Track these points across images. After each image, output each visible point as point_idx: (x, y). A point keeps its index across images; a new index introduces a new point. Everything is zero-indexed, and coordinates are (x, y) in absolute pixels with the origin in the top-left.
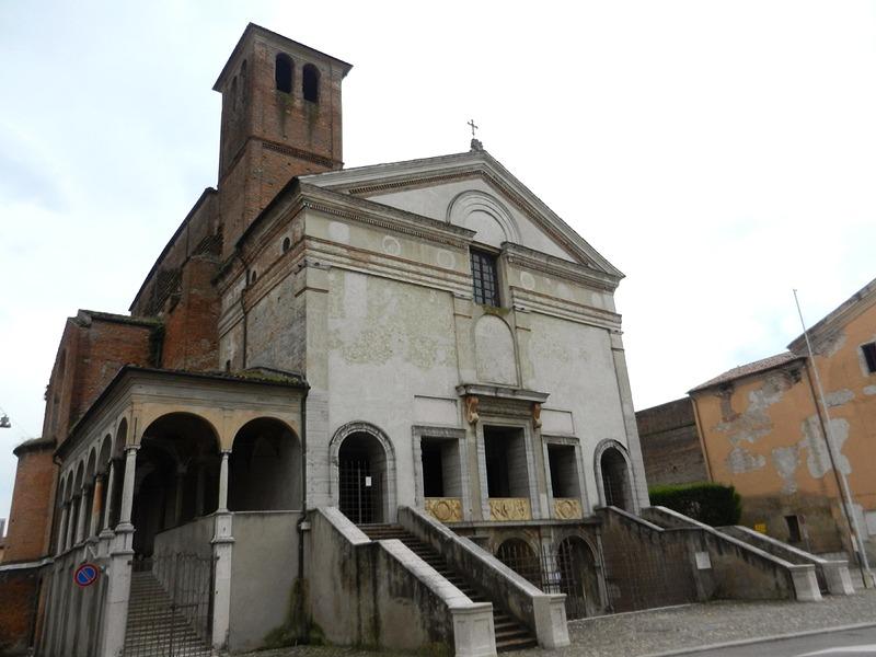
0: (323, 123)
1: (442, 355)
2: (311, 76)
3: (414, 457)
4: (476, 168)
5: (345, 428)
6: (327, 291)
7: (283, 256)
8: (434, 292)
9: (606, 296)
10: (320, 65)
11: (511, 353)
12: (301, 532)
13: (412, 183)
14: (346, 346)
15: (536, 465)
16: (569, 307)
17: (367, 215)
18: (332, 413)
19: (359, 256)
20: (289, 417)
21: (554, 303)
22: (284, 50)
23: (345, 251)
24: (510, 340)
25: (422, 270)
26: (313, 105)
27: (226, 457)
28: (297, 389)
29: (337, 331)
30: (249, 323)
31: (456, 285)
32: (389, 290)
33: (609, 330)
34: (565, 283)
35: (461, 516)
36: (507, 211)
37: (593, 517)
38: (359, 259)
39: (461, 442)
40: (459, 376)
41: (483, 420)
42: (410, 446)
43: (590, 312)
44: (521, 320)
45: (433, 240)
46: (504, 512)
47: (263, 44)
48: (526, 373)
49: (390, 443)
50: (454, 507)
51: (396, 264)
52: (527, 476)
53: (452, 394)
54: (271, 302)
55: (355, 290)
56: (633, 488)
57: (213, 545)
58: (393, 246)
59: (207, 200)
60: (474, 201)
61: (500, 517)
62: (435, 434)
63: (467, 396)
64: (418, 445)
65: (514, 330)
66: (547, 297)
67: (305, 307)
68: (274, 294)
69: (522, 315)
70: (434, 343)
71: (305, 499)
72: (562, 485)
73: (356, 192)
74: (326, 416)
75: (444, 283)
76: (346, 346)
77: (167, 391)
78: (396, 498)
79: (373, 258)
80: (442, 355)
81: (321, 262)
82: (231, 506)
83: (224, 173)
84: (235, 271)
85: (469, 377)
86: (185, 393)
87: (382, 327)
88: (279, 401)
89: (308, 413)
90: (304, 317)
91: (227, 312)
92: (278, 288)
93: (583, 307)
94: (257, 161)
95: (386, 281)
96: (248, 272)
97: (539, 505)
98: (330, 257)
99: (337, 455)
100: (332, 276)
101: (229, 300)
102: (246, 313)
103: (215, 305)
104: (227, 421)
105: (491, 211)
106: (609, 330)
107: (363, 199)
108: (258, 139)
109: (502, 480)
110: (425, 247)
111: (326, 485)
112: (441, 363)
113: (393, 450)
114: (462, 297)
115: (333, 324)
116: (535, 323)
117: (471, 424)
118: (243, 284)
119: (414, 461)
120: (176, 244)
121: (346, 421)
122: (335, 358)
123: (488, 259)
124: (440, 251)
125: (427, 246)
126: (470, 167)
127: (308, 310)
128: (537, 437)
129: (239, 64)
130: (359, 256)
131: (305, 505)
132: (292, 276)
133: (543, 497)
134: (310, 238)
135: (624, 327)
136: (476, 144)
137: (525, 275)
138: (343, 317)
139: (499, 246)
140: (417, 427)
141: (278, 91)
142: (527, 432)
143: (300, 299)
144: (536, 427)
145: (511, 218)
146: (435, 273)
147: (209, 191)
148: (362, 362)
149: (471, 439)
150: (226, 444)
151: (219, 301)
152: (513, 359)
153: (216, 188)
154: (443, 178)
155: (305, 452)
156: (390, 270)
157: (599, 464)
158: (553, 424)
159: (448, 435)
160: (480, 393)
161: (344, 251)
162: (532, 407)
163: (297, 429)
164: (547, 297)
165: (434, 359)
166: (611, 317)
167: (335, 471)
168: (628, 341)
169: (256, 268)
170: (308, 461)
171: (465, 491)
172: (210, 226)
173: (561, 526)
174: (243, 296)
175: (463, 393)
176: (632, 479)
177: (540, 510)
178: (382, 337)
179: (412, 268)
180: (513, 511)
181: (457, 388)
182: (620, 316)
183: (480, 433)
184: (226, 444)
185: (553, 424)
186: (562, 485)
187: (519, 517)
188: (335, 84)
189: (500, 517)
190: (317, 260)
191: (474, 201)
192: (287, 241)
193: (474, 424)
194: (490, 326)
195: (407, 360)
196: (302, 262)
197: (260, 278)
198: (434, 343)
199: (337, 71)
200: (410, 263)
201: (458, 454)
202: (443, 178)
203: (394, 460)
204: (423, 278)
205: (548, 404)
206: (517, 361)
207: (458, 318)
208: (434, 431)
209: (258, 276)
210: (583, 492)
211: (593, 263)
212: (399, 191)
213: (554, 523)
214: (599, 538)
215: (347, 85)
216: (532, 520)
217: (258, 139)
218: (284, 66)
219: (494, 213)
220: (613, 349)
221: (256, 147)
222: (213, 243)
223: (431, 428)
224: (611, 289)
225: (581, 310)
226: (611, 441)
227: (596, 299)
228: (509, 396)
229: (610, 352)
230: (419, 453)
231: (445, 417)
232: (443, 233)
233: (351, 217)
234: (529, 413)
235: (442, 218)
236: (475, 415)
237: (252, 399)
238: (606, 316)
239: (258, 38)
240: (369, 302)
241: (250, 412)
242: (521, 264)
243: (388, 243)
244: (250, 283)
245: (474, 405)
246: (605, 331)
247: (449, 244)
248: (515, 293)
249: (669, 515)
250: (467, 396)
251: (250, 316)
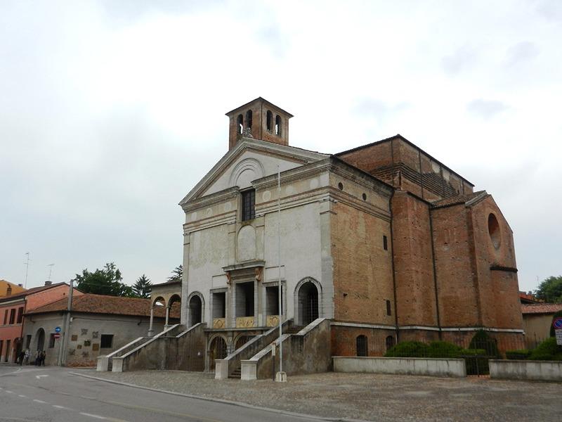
16: (288, 200)
20: (178, 293)
32: (207, 233)
39: (226, 293)
43: (304, 196)
53: (222, 272)
69: (260, 219)
72: (274, 309)
97: (261, 318)
123: (247, 196)
124: (225, 204)
133: (260, 316)
146: (219, 218)
154: (228, 165)
158: (269, 276)
159: (221, 291)
161: (192, 225)
166: (320, 192)
183: (234, 288)
185: (269, 276)
189: (242, 326)
195: (211, 262)
202: (228, 165)
211: (310, 159)
220: (321, 214)
226: (306, 278)
228: (241, 268)
231: (222, 283)
233: (197, 208)
237: (171, 289)
242: (263, 188)
246: (318, 203)
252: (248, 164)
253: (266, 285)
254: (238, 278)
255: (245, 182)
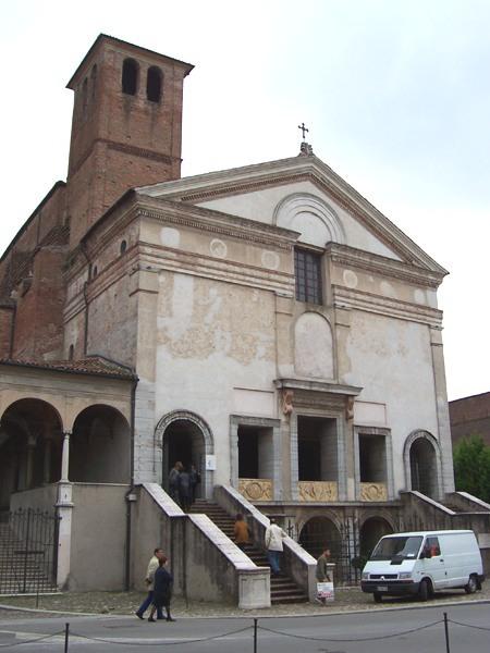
0: (164, 122)
1: (261, 350)
2: (155, 78)
3: (231, 442)
4: (304, 171)
5: (169, 415)
6: (157, 293)
7: (120, 258)
8: (256, 292)
9: (429, 293)
10: (162, 66)
11: (331, 348)
12: (129, 502)
13: (242, 188)
14: (173, 342)
15: (346, 453)
16: (390, 303)
17: (197, 221)
18: (157, 403)
19: (189, 259)
20: (121, 406)
21: (375, 300)
22: (131, 55)
23: (174, 255)
24: (328, 337)
25: (248, 271)
26: (156, 105)
27: (67, 437)
28: (127, 380)
29: (166, 329)
30: (90, 314)
31: (279, 285)
33: (429, 326)
34: (388, 280)
35: (272, 496)
36: (333, 212)
37: (397, 501)
38: (187, 261)
39: (275, 430)
40: (277, 369)
41: (296, 411)
42: (227, 433)
43: (411, 308)
44: (341, 317)
45: (261, 243)
46: (313, 493)
47: (111, 52)
48: (343, 367)
49: (209, 430)
50: (266, 487)
51: (223, 266)
52: (337, 463)
53: (268, 386)
54: (108, 298)
55: (183, 290)
56: (439, 475)
57: (57, 507)
58: (220, 249)
59: (57, 192)
60: (300, 203)
61: (309, 498)
62: (251, 423)
63: (283, 388)
64: (235, 432)
65: (333, 326)
66: (368, 294)
67: (137, 306)
68: (112, 291)
69: (343, 312)
70: (254, 340)
71: (132, 475)
73: (186, 199)
74: (152, 405)
75: (268, 283)
76: (173, 342)
77: (19, 381)
78: (212, 479)
79: (201, 261)
80: (261, 350)
81: (153, 265)
82: (71, 478)
83: (75, 165)
84: (80, 264)
85: (287, 371)
86: (36, 382)
87: (206, 325)
88: (111, 391)
89: (137, 401)
90: (136, 315)
91: (73, 300)
92: (115, 286)
93: (404, 303)
94: (101, 161)
95: (212, 282)
96: (91, 265)
97: (346, 489)
98: (161, 260)
99: (161, 438)
100: (162, 278)
101: (74, 288)
102: (88, 304)
103: (62, 292)
104: (69, 407)
105: (316, 212)
106: (429, 326)
107: (193, 208)
108: (104, 141)
109: (313, 465)
110: (250, 249)
111: (151, 464)
112: (260, 358)
113: (211, 437)
114: (284, 296)
115: (162, 322)
116: (355, 319)
117: (286, 415)
118: (84, 278)
119: (231, 447)
120: (29, 228)
121: (169, 410)
122: (162, 353)
123: (311, 260)
124: (265, 252)
125: (253, 248)
126: (299, 170)
127: (139, 310)
128: (350, 427)
129: (90, 68)
130: (189, 259)
131: (132, 480)
132: (127, 276)
133: (351, 482)
134: (144, 244)
135: (445, 323)
136: (305, 148)
137: (347, 273)
138: (171, 315)
139: (323, 246)
140: (235, 416)
141: (126, 91)
142: (340, 422)
143: (133, 299)
144: (349, 418)
145: (337, 218)
146: (259, 273)
147: (59, 185)
148: (187, 357)
149: (285, 429)
150: (68, 426)
151: (65, 288)
152: (330, 354)
153: (65, 181)
155: (133, 435)
156: (215, 272)
157: (408, 452)
158: (364, 415)
159: (264, 424)
160: (296, 386)
162: (346, 400)
163: (127, 416)
164: (368, 294)
165: (254, 354)
166: (432, 313)
167: (159, 453)
168: (447, 337)
169: (99, 264)
170: (136, 443)
171: (277, 474)
172: (59, 217)
173: (365, 507)
174: (85, 289)
175: (280, 386)
176: (439, 467)
177: (346, 493)
178: (206, 334)
179: (237, 269)
180: (321, 493)
181: (274, 381)
182: (442, 312)
183: (294, 423)
184: (68, 426)
185: (364, 415)
186: (371, 469)
187: (326, 498)
188: (177, 84)
189: (309, 498)
190: (149, 264)
191: (300, 203)
192: (124, 242)
193: (288, 414)
194: (311, 325)
195: (229, 355)
196: (135, 266)
197: (102, 273)
198: (254, 340)
199: (179, 71)
200: (234, 264)
201: (272, 441)
203: (213, 445)
204: (248, 278)
205: (362, 396)
206: (335, 356)
207: (278, 316)
208: (250, 421)
209: (98, 271)
210: (389, 478)
211: (417, 260)
212: (228, 196)
213: (359, 504)
214: (401, 519)
215: (190, 84)
216: (339, 501)
217: (104, 141)
218: (130, 69)
219: (319, 214)
220: (432, 344)
221: (101, 148)
222: (61, 234)
223: (248, 418)
224: (435, 286)
225: (402, 306)
226: (421, 431)
227: (419, 296)
228: (323, 390)
229: (429, 348)
230: (236, 439)
231: (261, 407)
232: (268, 235)
233: (181, 223)
234: (343, 405)
235: (267, 220)
236: (290, 407)
237: (90, 389)
238: (427, 312)
239: (108, 47)
240: (196, 302)
241: (87, 400)
242: (344, 263)
243: (216, 245)
244: (92, 277)
245: (289, 397)
246: (426, 327)
247: (273, 245)
248: (337, 291)
249: (469, 500)
250: (283, 388)
251: (91, 307)
252: (328, 215)
253: (359, 430)
254: (303, 405)
255: (314, 234)
